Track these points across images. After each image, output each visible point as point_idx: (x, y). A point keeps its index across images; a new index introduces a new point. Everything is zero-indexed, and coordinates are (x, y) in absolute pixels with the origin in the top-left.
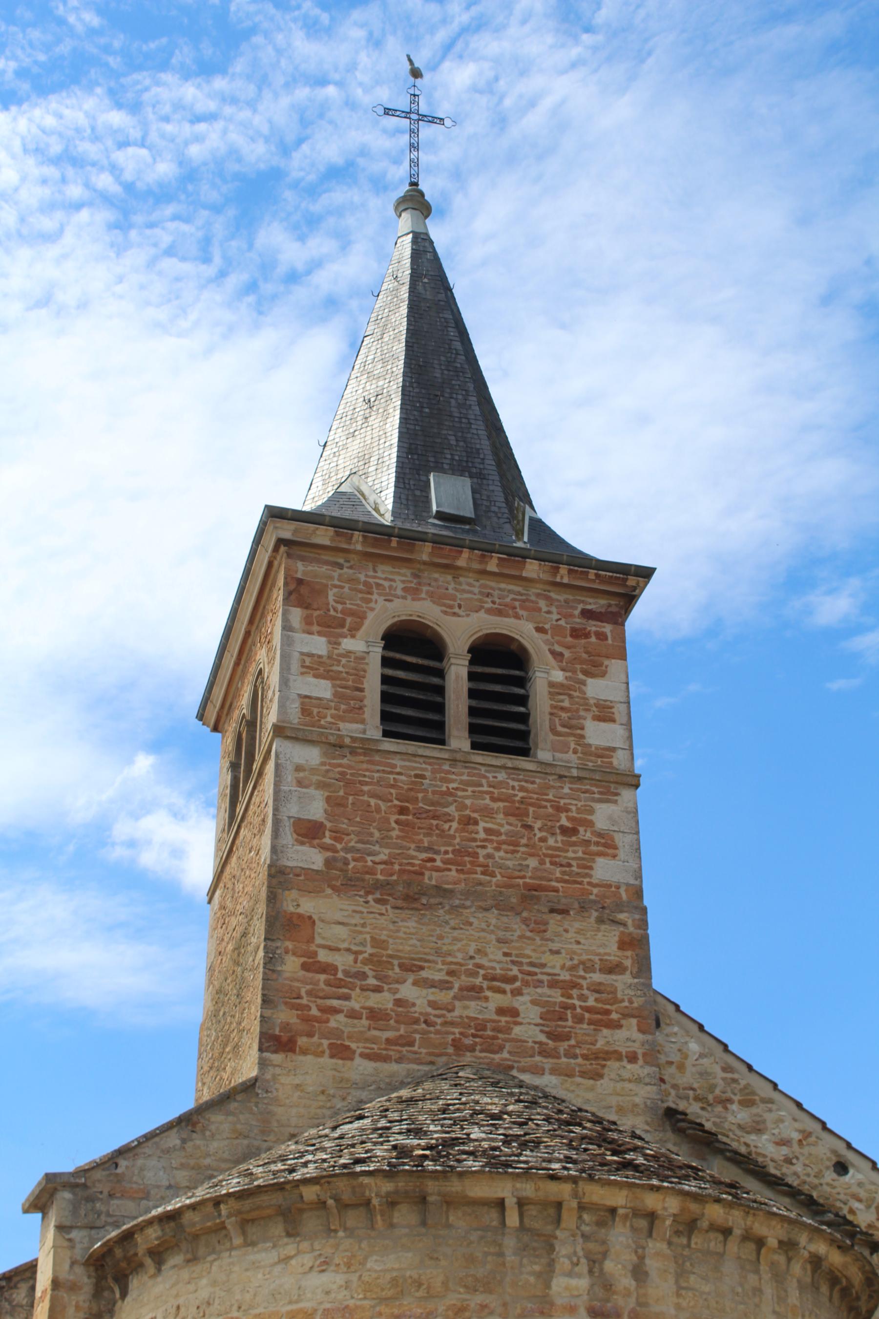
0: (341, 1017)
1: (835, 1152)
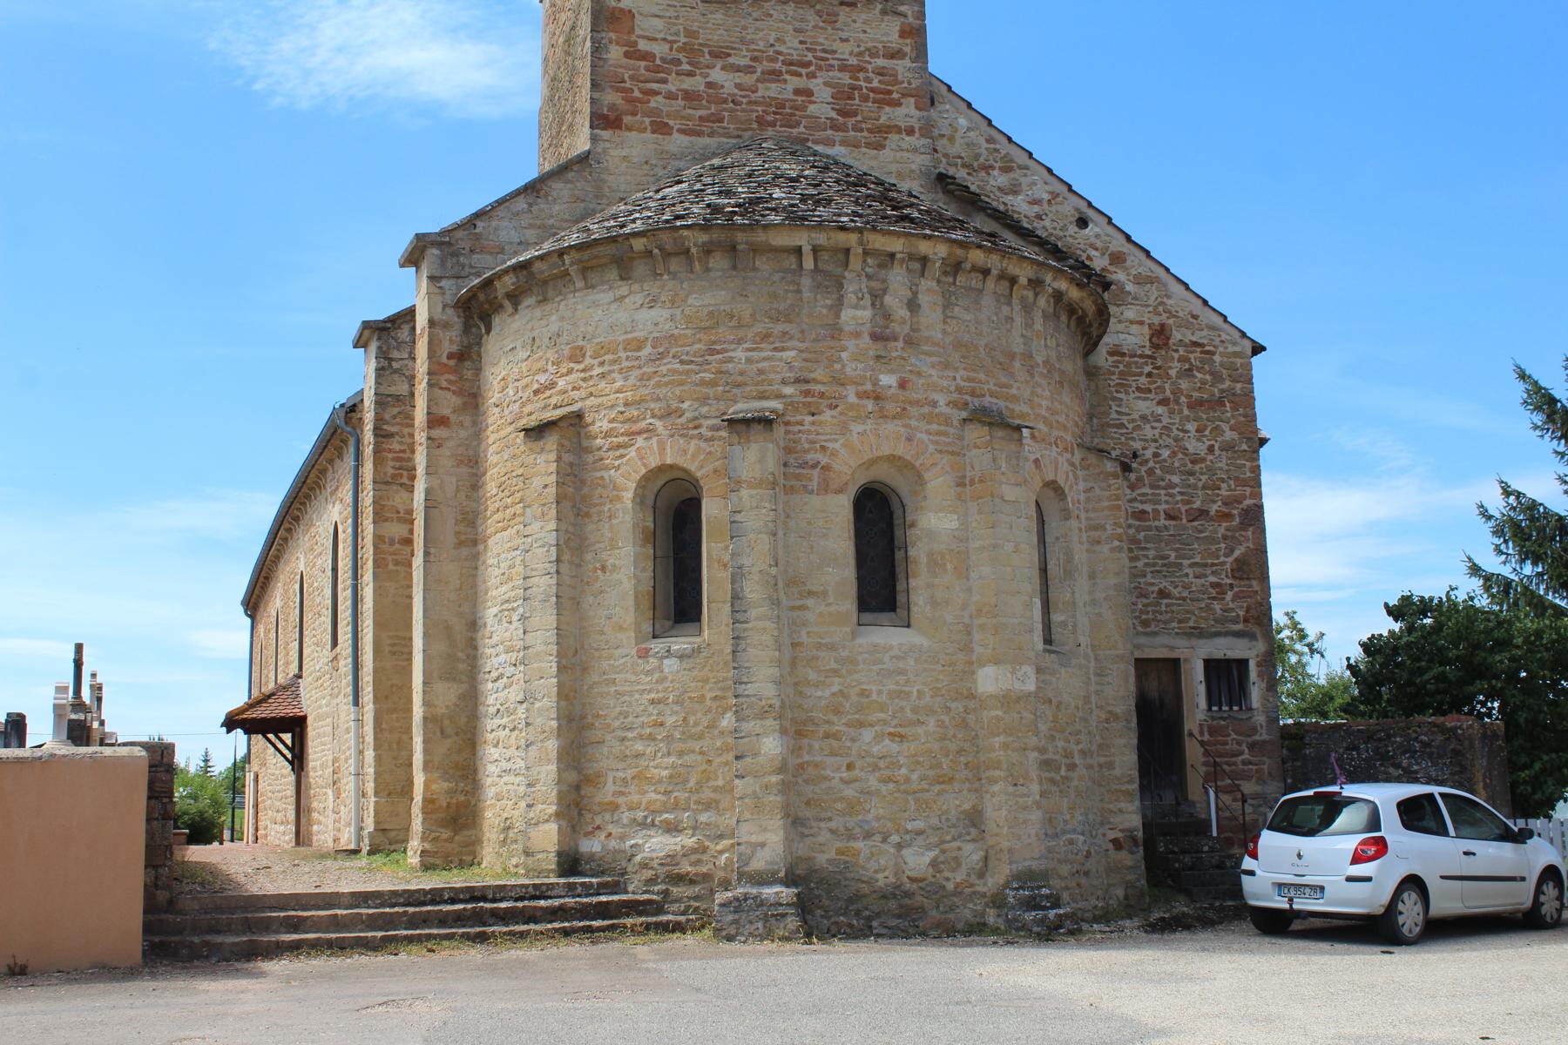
0: (659, 98)
1: (1077, 210)
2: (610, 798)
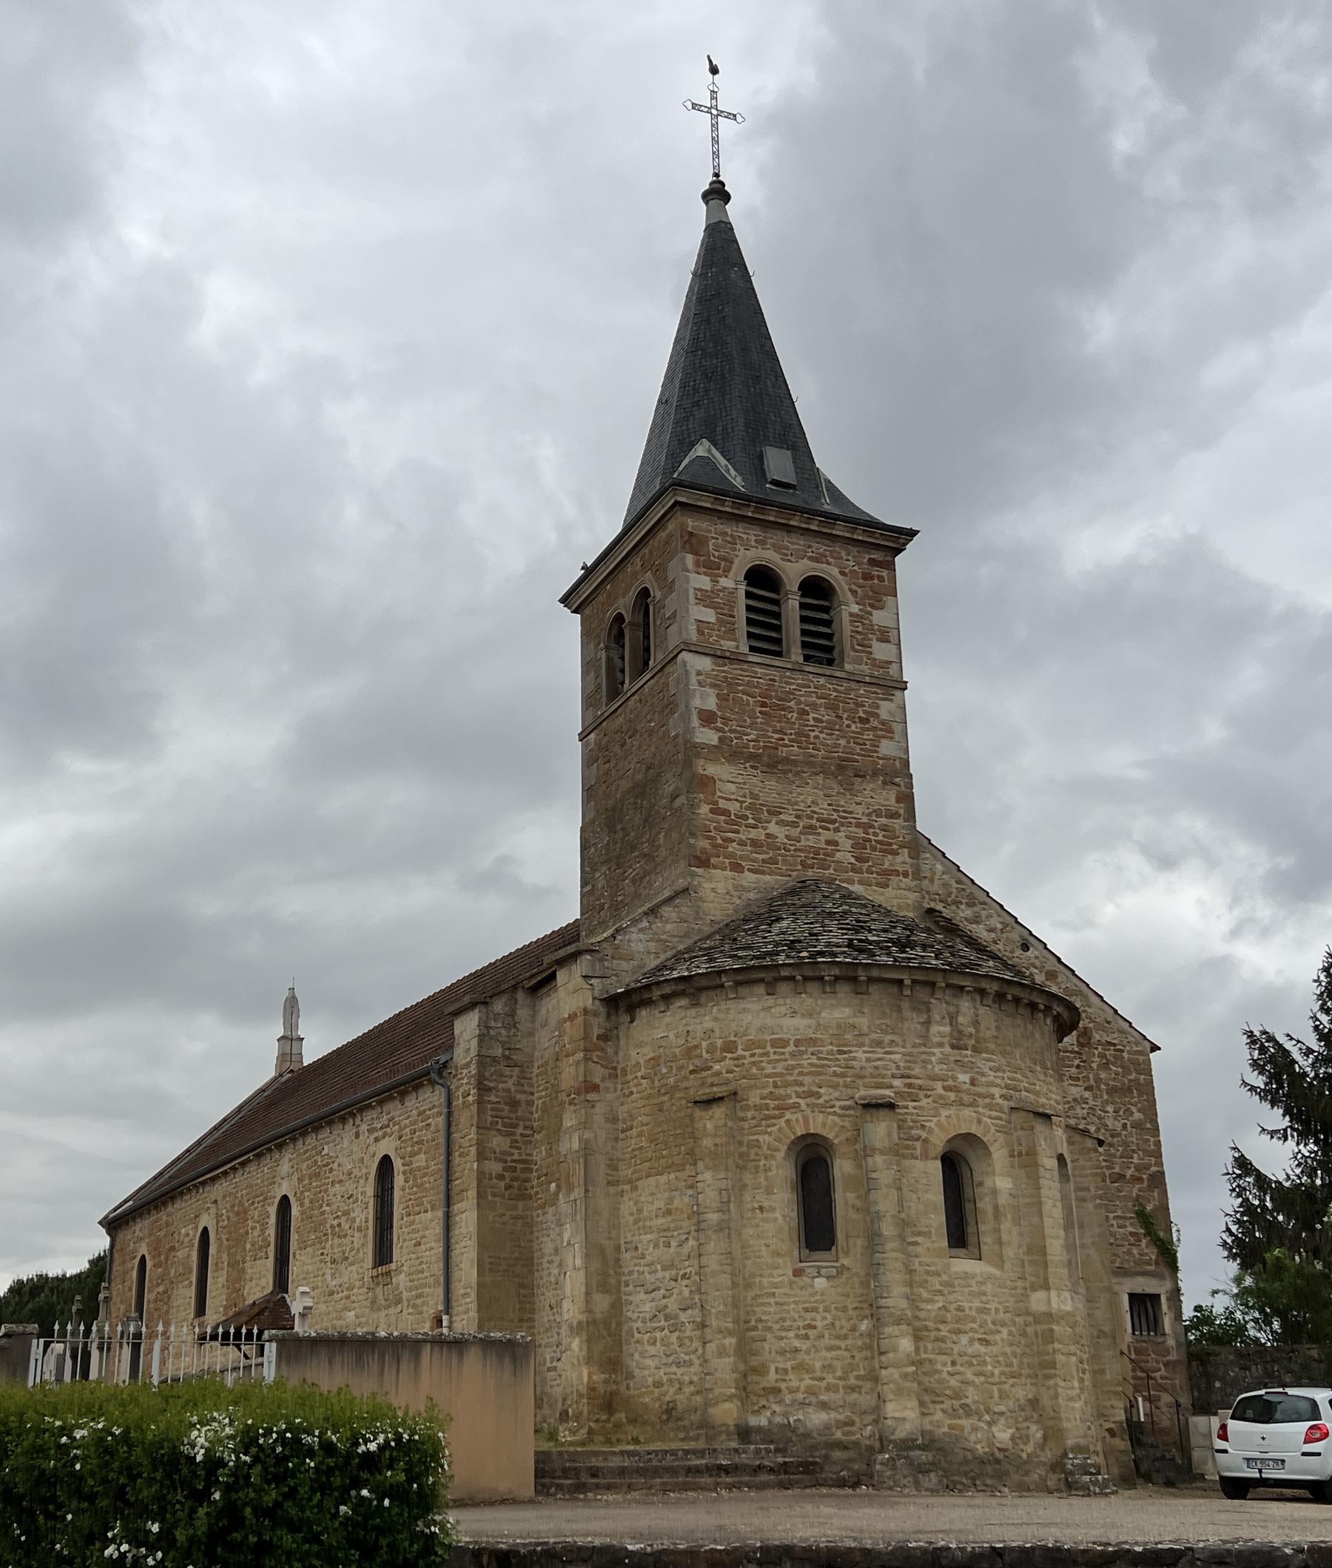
0: (734, 844)
2: (773, 1384)
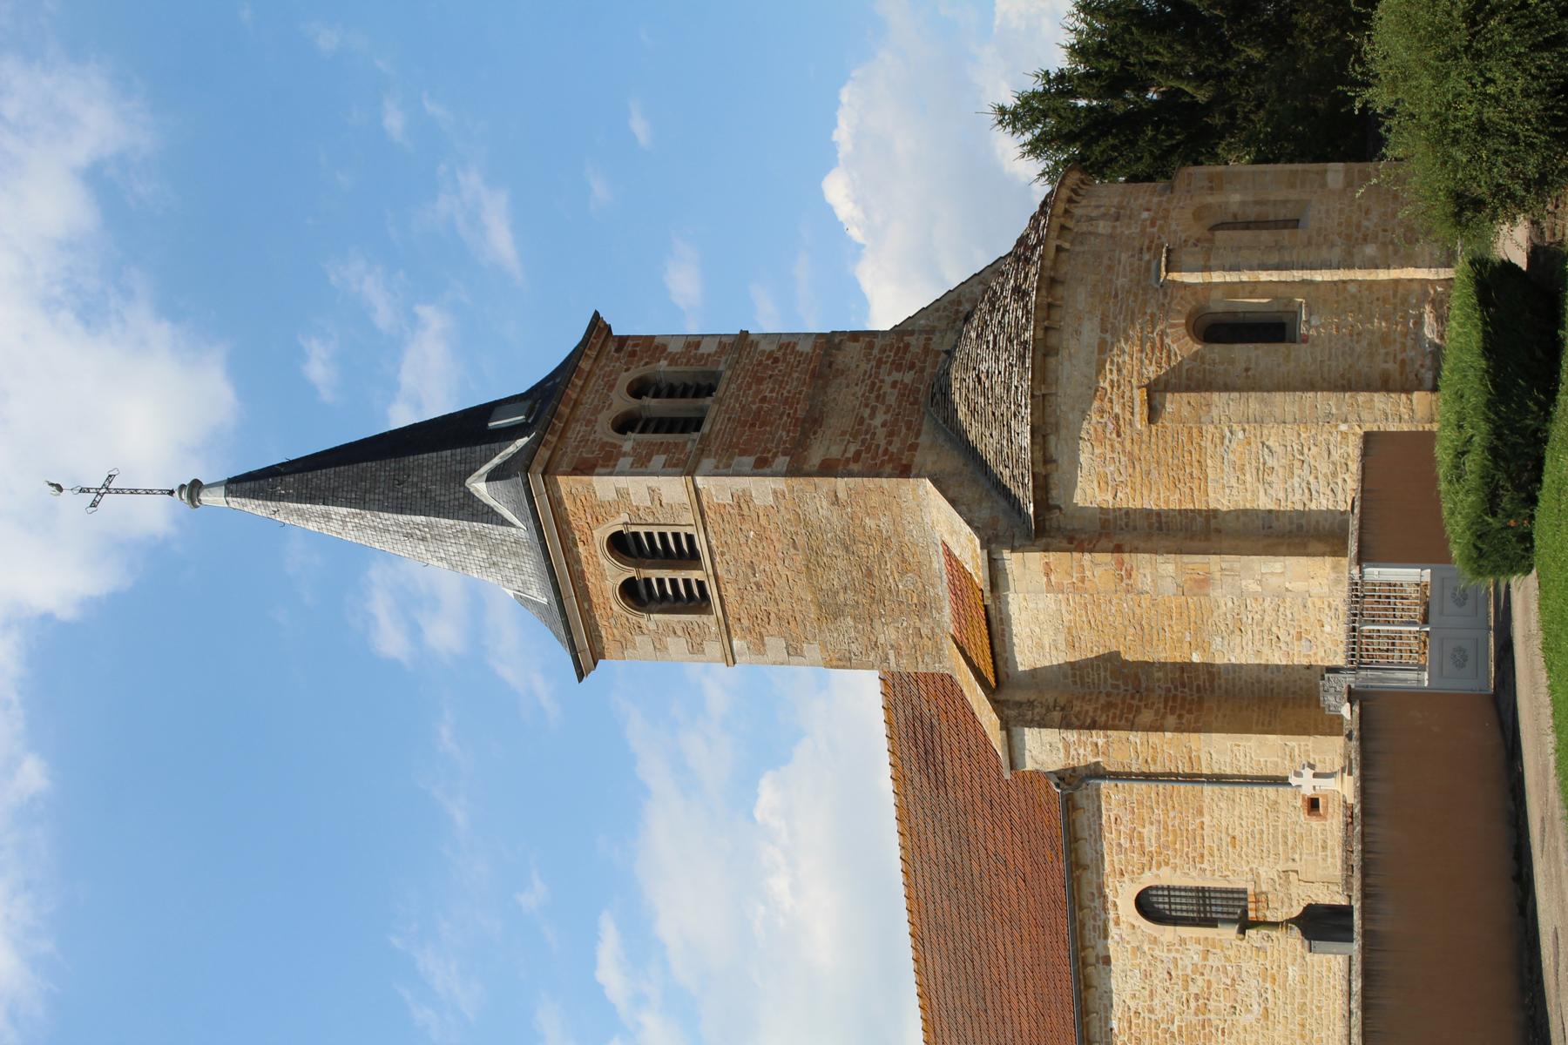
2: (1397, 366)
